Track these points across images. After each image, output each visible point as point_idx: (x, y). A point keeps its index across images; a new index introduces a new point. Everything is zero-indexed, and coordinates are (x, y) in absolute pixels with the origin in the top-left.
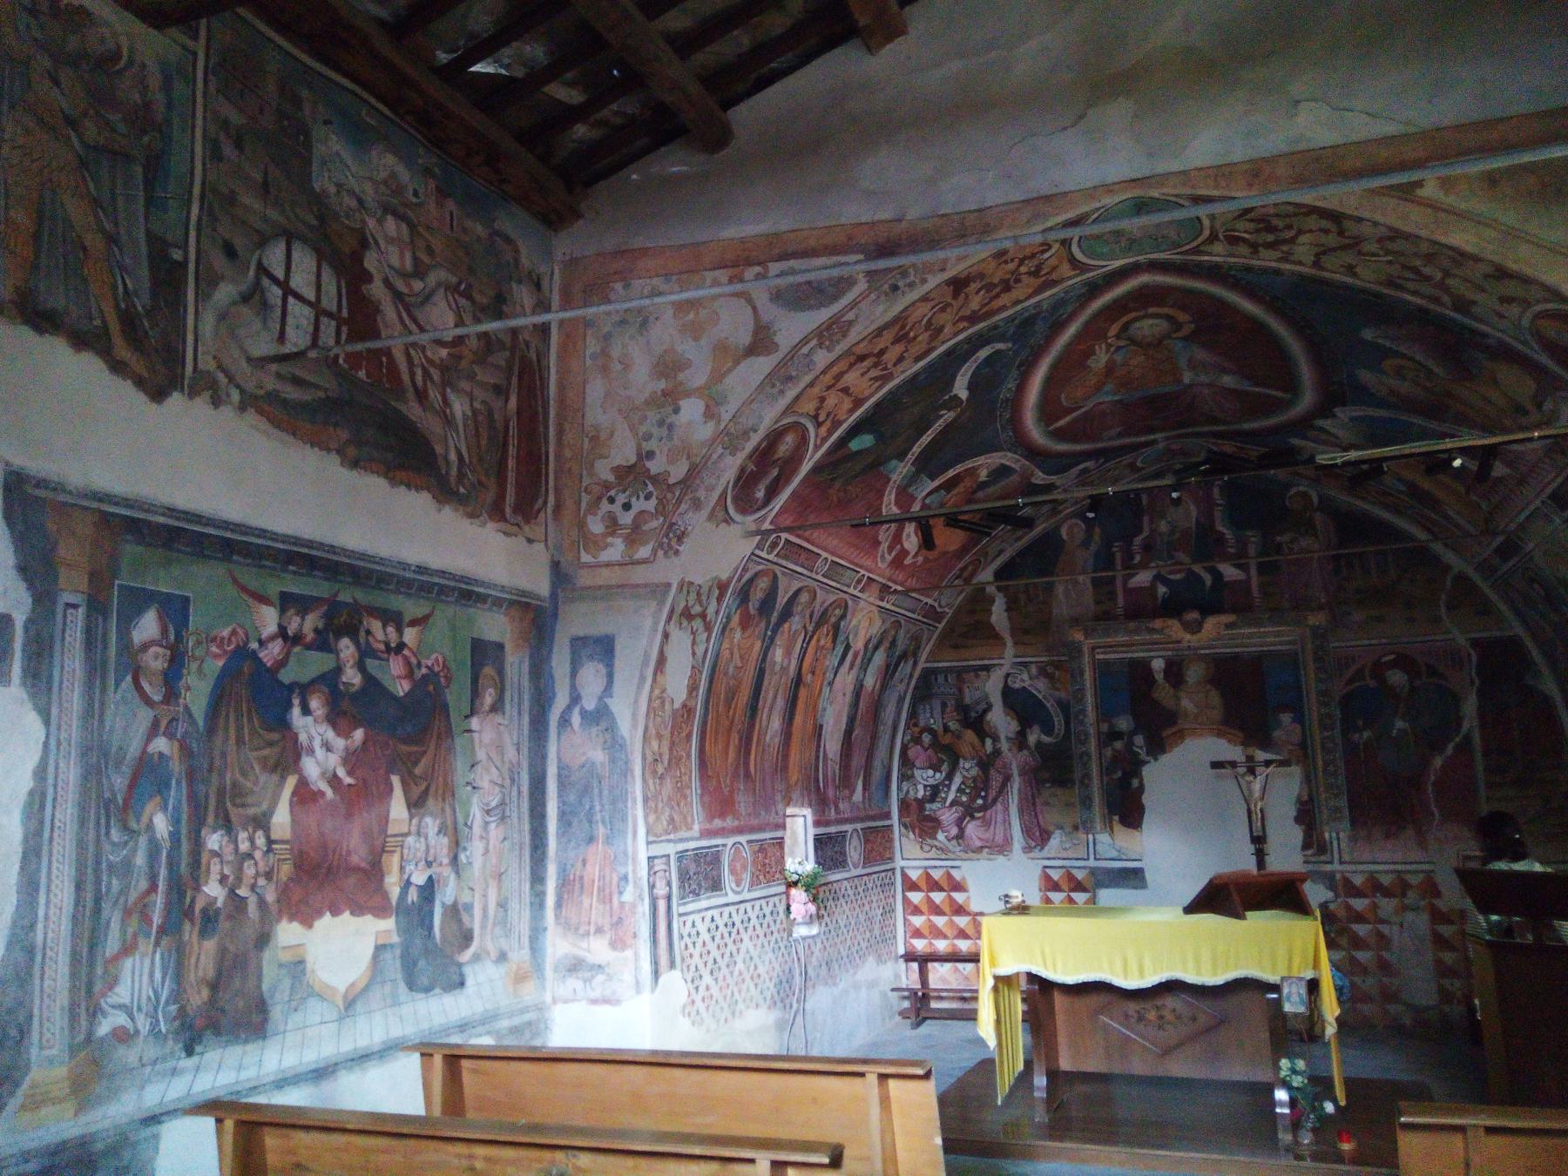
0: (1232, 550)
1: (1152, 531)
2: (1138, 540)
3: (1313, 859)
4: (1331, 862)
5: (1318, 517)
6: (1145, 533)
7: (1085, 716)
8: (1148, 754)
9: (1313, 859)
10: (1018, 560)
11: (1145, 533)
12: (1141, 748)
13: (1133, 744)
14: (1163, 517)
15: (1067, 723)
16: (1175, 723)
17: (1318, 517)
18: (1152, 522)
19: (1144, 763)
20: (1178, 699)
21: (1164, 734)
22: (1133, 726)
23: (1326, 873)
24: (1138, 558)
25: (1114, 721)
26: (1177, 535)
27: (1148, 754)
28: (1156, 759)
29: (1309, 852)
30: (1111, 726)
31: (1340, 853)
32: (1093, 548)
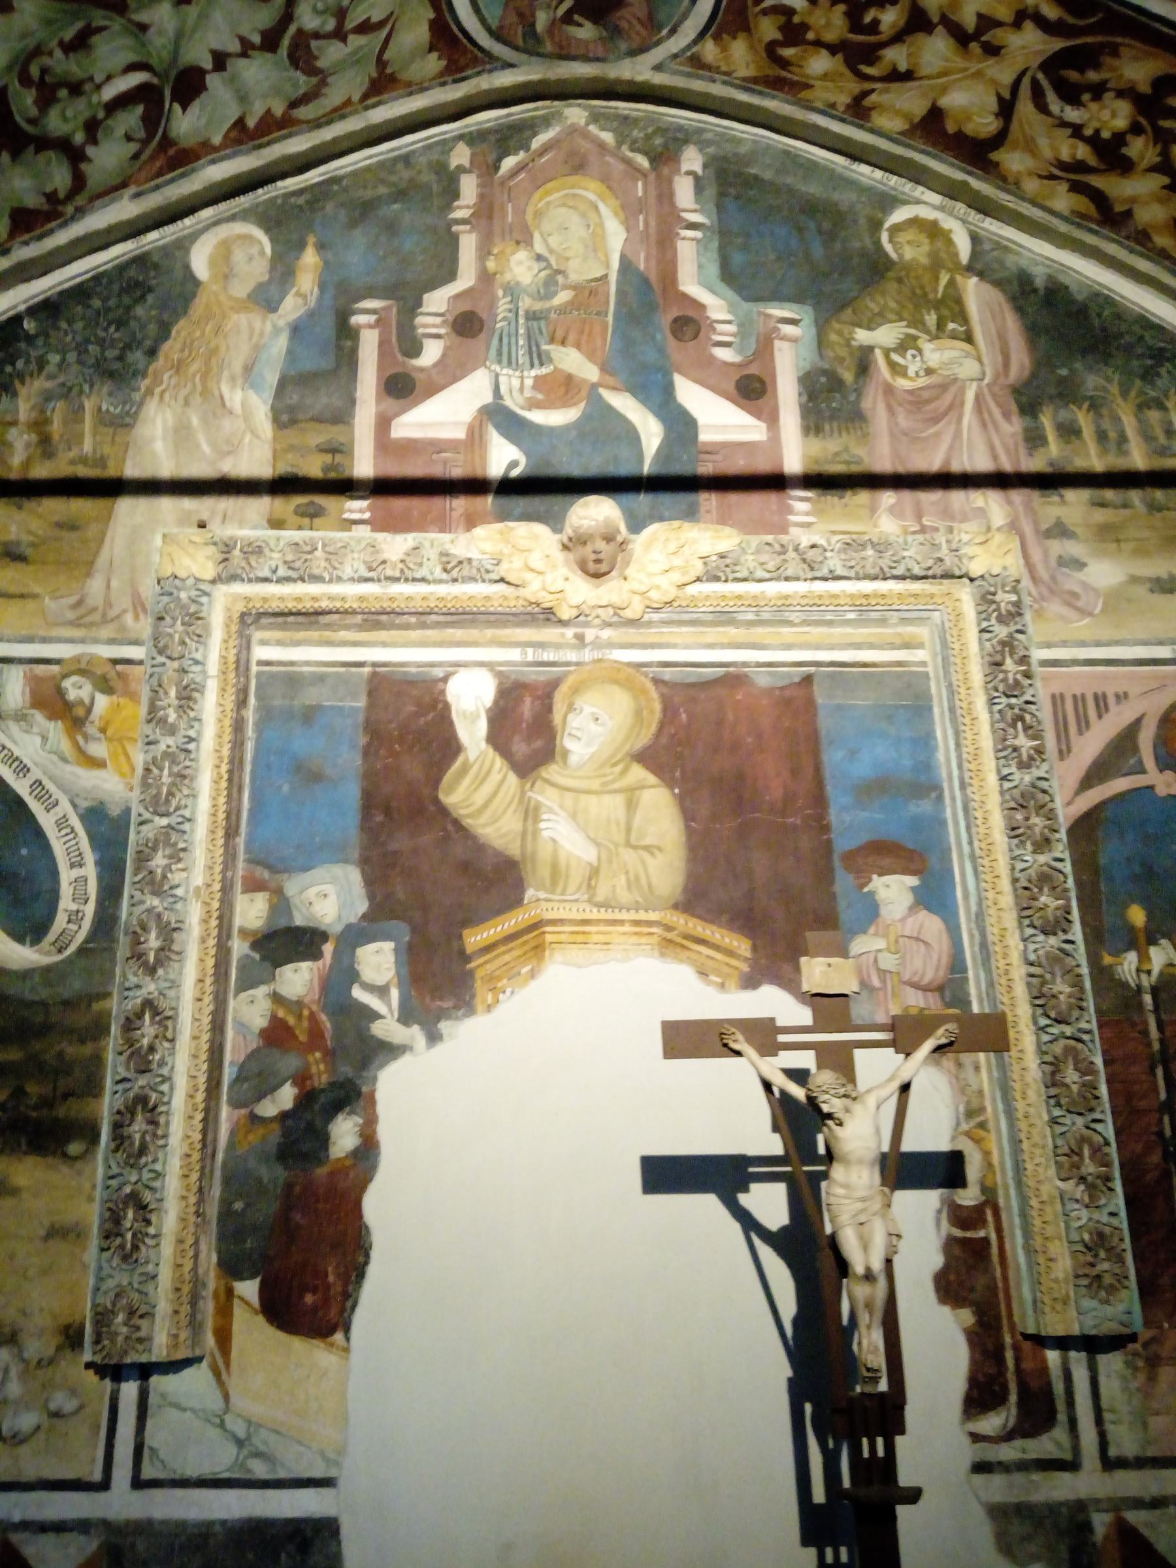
0: (725, 355)
1: (486, 278)
2: (438, 301)
3: (1008, 1452)
4: (1072, 1466)
5: (973, 291)
6: (466, 279)
7: (177, 855)
8: (406, 1018)
9: (1008, 1452)
10: (29, 325)
11: (466, 279)
12: (381, 991)
13: (353, 976)
14: (524, 239)
15: (110, 892)
16: (513, 899)
17: (973, 291)
18: (484, 252)
19: (391, 1051)
20: (531, 814)
21: (474, 938)
22: (362, 906)
23: (1053, 1509)
24: (431, 353)
25: (292, 886)
26: (562, 297)
27: (406, 1018)
28: (434, 1037)
29: (991, 1423)
30: (280, 903)
31: (1099, 1421)
32: (291, 308)
